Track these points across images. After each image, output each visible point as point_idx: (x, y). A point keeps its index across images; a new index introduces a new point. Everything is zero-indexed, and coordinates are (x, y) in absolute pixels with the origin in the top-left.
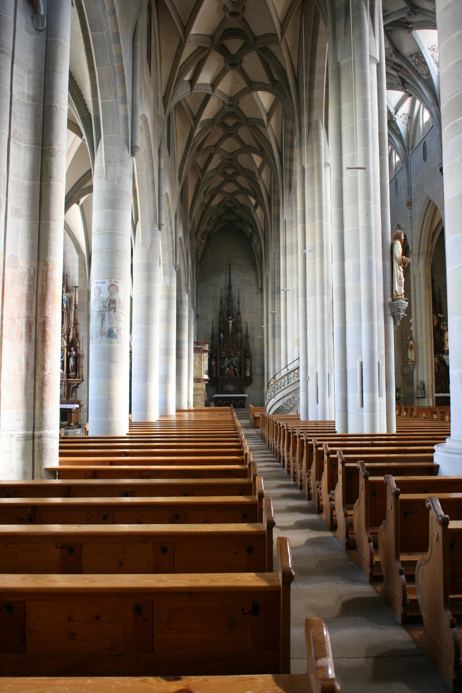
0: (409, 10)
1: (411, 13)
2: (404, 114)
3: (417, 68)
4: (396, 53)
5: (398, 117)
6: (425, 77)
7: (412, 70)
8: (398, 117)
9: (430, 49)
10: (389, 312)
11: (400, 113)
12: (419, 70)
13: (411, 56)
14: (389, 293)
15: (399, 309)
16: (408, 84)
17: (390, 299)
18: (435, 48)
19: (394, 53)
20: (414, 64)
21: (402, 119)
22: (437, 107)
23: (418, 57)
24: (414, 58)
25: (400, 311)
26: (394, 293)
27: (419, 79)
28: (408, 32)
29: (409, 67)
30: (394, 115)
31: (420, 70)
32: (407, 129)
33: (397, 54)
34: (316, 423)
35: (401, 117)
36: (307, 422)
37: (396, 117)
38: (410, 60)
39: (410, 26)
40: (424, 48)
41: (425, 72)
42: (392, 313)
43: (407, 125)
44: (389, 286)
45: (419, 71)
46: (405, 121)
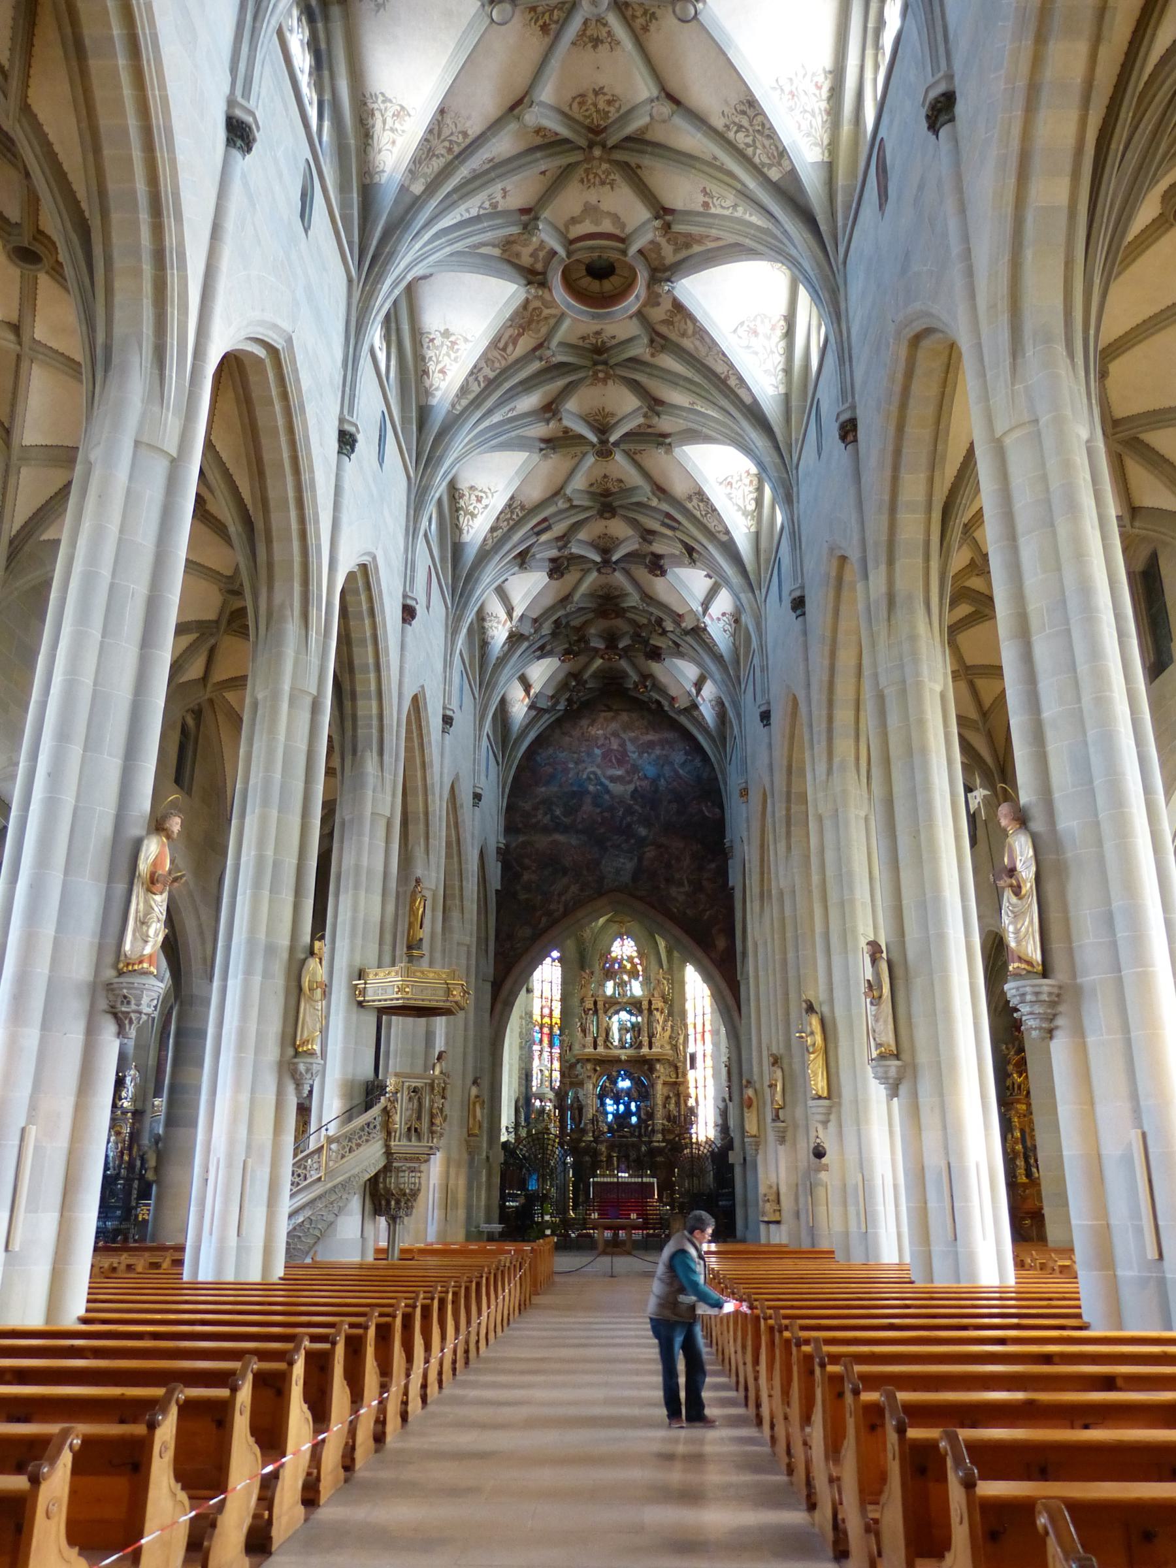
0: (645, 409)
1: (650, 414)
2: (724, 614)
3: (705, 521)
4: (658, 493)
5: (712, 619)
6: (724, 538)
7: (694, 524)
8: (712, 619)
9: (721, 483)
10: (103, 1004)
11: (716, 609)
12: (709, 525)
13: (690, 498)
14: (109, 959)
15: (125, 997)
16: (698, 552)
17: (109, 974)
18: (734, 481)
19: (654, 494)
20: (698, 514)
21: (721, 624)
22: (750, 595)
23: (702, 501)
24: (695, 502)
25: (129, 1003)
26: (122, 958)
27: (711, 542)
28: (666, 453)
29: (687, 518)
30: (701, 617)
31: (711, 524)
32: (734, 644)
33: (662, 496)
34: (218, 1286)
35: (719, 619)
36: (195, 1286)
37: (707, 620)
38: (689, 506)
39: (668, 441)
40: (706, 481)
41: (720, 528)
42: (112, 1007)
43: (734, 635)
44: (111, 941)
45: (711, 526)
46: (727, 627)
